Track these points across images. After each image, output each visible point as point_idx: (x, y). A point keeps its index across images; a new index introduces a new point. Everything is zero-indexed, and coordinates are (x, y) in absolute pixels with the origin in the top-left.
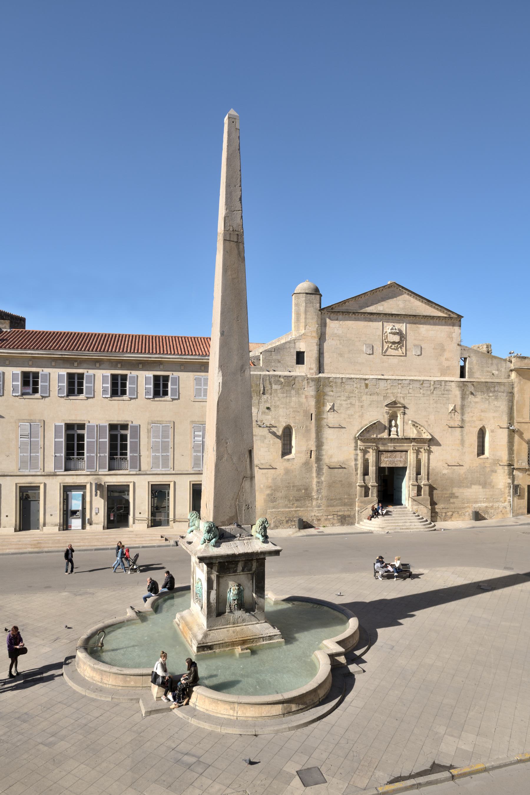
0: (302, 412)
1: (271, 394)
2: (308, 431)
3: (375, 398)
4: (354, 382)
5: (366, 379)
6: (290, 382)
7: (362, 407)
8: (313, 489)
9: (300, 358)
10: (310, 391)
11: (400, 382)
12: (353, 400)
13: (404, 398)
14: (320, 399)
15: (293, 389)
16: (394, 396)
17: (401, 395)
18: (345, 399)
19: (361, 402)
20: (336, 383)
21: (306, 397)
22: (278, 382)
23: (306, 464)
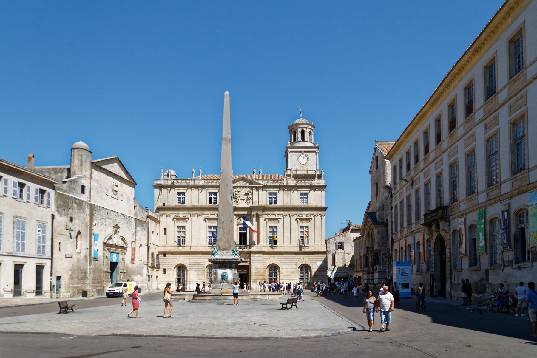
2: (87, 236)
10: (88, 211)
12: (102, 221)
14: (92, 215)
22: (76, 203)
23: (86, 256)
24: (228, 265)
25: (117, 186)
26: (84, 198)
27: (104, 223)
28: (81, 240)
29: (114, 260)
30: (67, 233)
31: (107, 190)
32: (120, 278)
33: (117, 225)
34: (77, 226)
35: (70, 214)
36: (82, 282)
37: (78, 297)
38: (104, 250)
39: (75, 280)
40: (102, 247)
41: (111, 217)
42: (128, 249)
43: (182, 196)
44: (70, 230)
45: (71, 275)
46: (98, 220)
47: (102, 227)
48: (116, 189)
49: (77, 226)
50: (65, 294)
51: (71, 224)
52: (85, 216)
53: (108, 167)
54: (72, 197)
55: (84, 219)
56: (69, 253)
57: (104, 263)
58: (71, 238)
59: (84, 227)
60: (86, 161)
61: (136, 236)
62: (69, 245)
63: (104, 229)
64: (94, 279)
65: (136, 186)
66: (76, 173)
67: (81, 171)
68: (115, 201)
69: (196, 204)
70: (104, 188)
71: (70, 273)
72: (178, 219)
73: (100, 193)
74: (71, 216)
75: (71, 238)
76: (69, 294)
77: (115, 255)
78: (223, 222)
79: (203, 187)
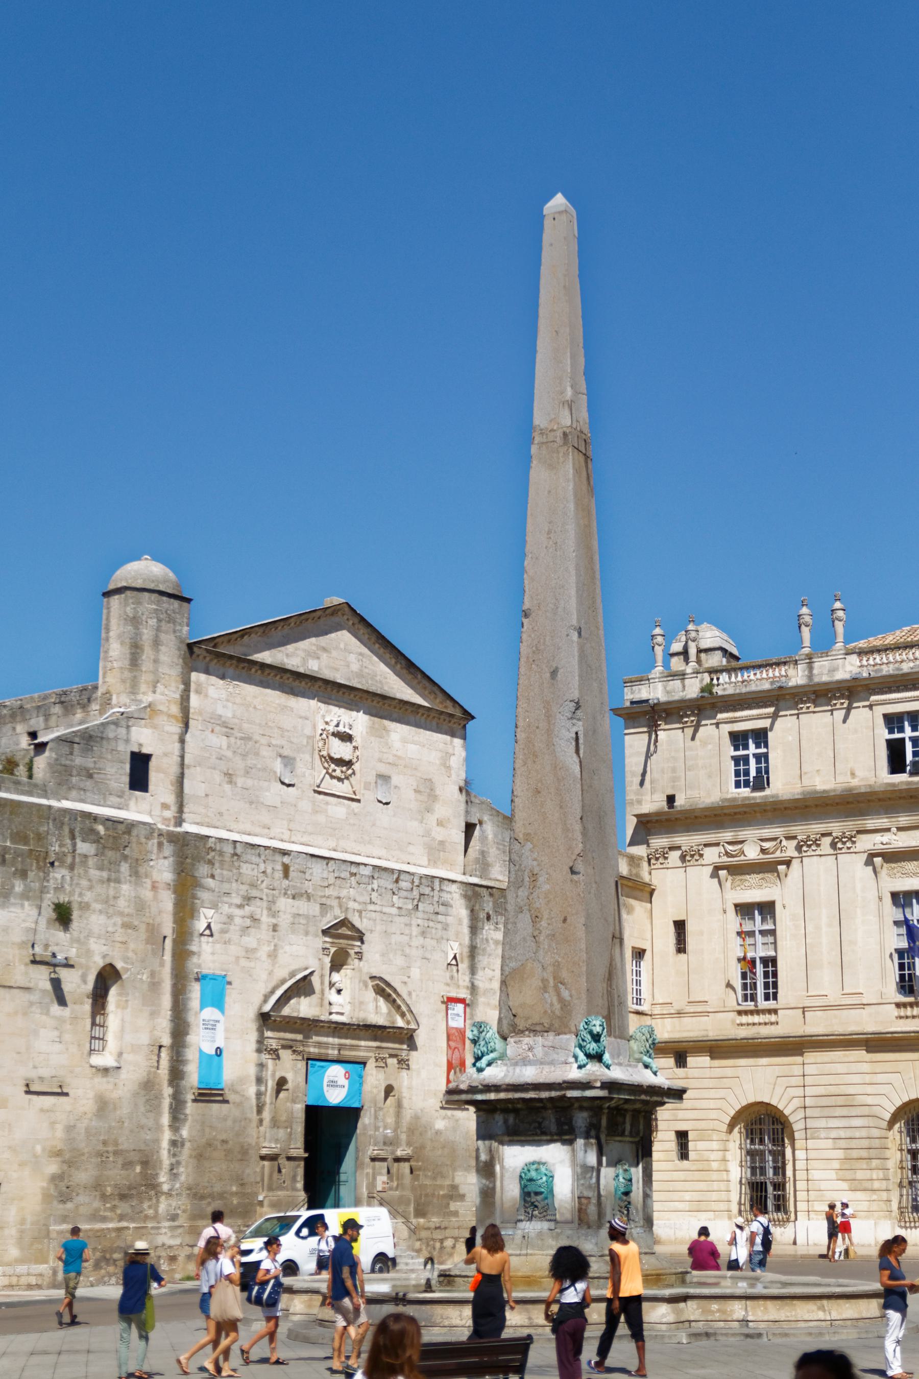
0: (143, 927)
1: (72, 868)
2: (155, 985)
3: (302, 906)
4: (259, 855)
5: (285, 853)
6: (117, 839)
7: (275, 928)
8: (161, 1162)
9: (139, 771)
10: (162, 869)
11: (354, 869)
12: (258, 909)
13: (360, 912)
15: (125, 858)
16: (340, 906)
17: (356, 906)
18: (238, 901)
19: (274, 916)
20: (221, 853)
21: (154, 887)
22: (90, 835)
23: (148, 1085)
24: (550, 1120)
25: (346, 738)
26: (140, 810)
27: (265, 919)
28: (122, 1006)
29: (335, 1097)
30: (41, 978)
31: (288, 761)
32: (372, 1185)
33: (344, 923)
34: (96, 940)
35: (59, 889)
36: (124, 1207)
37: (101, 1282)
38: (261, 1046)
39: (82, 1199)
40: (253, 1036)
41: (309, 887)
42: (421, 1038)
43: (752, 749)
44: (51, 963)
45: (56, 1179)
46: (225, 909)
47: (250, 941)
48: (340, 750)
49: (96, 940)
50: (22, 1269)
51: (61, 936)
52: (147, 894)
53: (295, 656)
54: (66, 811)
55: (140, 906)
56: (45, 1072)
57: (266, 1115)
58: (61, 1000)
59: (137, 944)
60: (156, 643)
61: (473, 970)
62: (48, 1034)
63: (266, 949)
64: (196, 1194)
65: (470, 725)
66: (114, 700)
67: (134, 689)
68: (339, 810)
69: (823, 781)
70: (265, 752)
71: (53, 1168)
72: (739, 870)
73: (240, 781)
74: (63, 899)
75: (61, 1000)
76: (43, 1268)
77: (336, 1072)
78: (534, 877)
79: (852, 692)
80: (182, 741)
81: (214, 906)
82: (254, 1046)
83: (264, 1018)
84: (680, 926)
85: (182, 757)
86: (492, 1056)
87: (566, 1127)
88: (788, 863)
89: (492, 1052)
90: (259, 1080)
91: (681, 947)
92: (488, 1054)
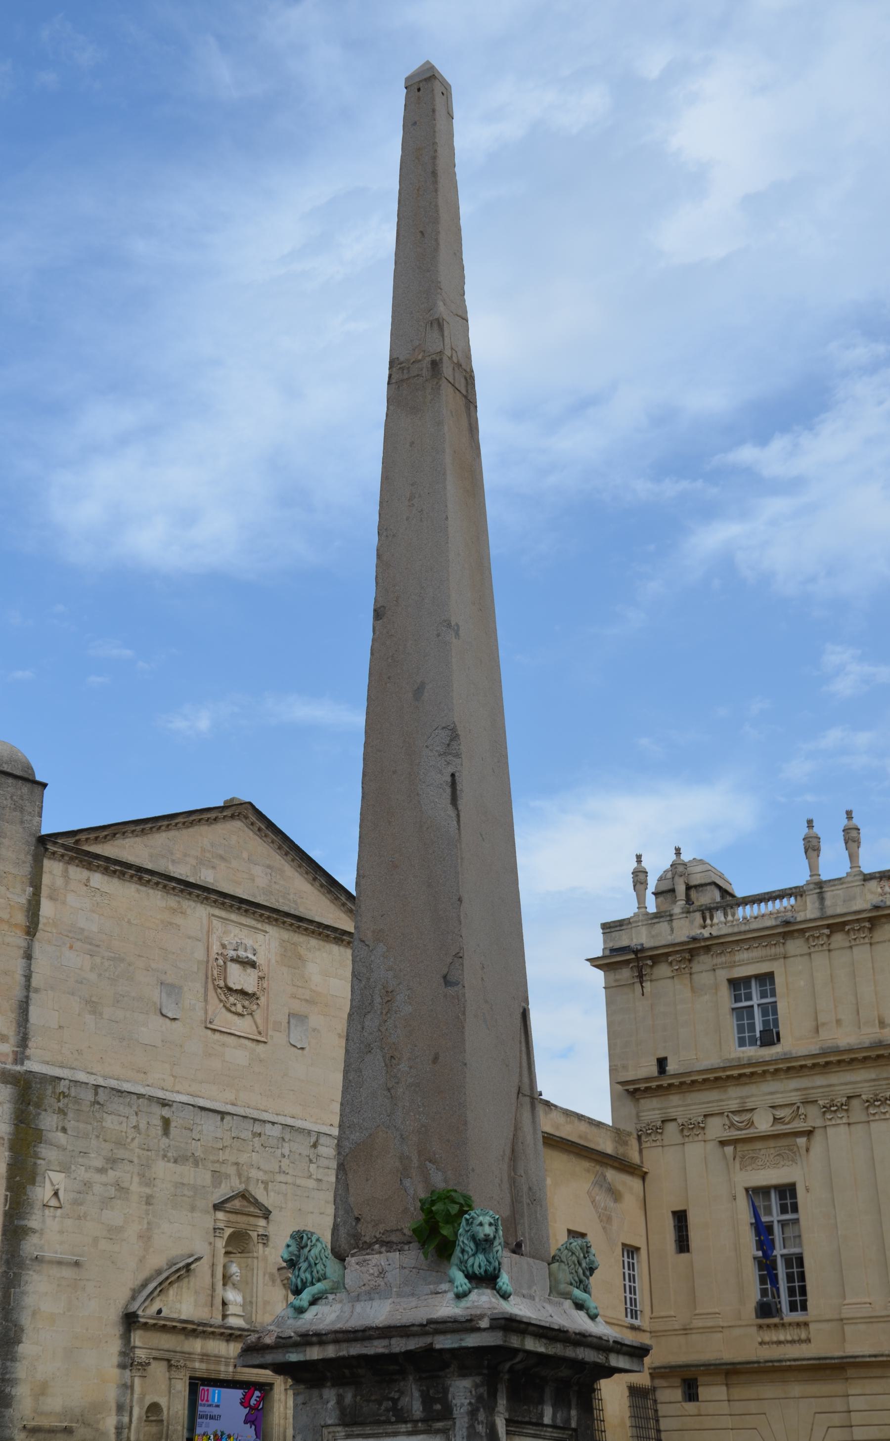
3: (188, 1173)
4: (130, 1105)
5: (164, 1103)
7: (149, 1200)
13: (266, 1183)
17: (260, 1175)
18: (99, 1163)
19: (147, 1185)
27: (135, 1187)
33: (244, 1196)
38: (128, 1361)
40: (115, 1346)
46: (81, 1173)
47: (114, 1216)
80: (28, 956)
81: (65, 1169)
82: (115, 1360)
83: (130, 1321)
84: (681, 1218)
85: (28, 977)
86: (319, 1286)
87: (438, 1407)
88: (809, 1133)
89: (319, 1280)
90: (120, 1408)
91: (683, 1244)
92: (313, 1284)
